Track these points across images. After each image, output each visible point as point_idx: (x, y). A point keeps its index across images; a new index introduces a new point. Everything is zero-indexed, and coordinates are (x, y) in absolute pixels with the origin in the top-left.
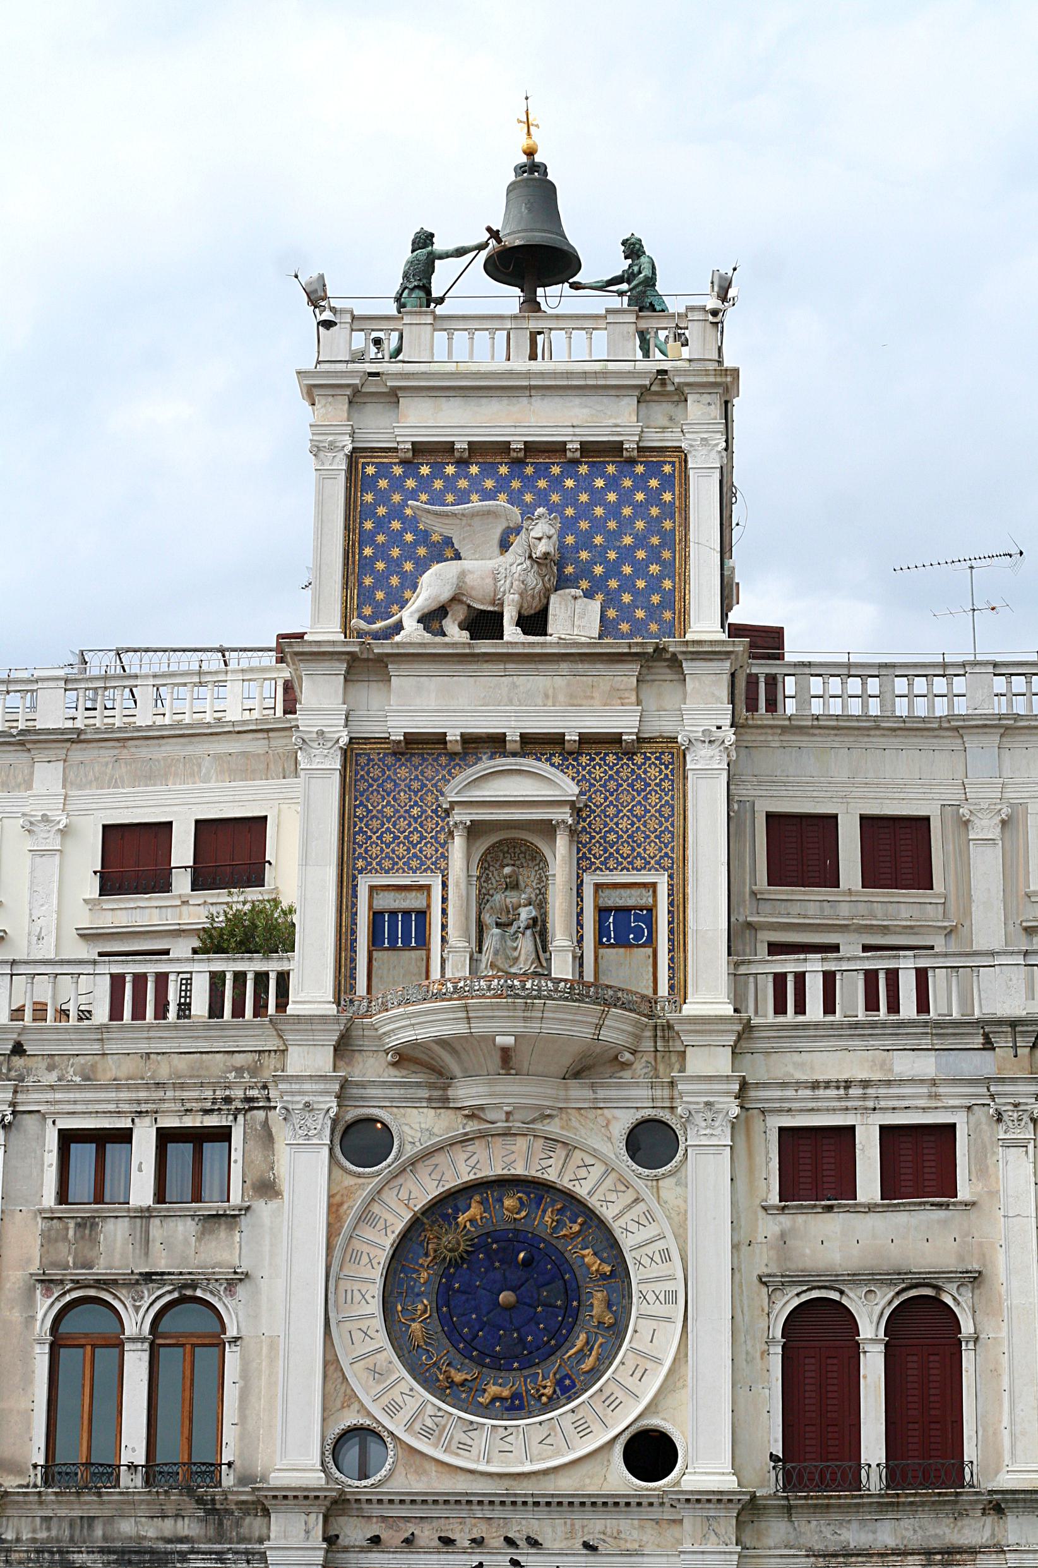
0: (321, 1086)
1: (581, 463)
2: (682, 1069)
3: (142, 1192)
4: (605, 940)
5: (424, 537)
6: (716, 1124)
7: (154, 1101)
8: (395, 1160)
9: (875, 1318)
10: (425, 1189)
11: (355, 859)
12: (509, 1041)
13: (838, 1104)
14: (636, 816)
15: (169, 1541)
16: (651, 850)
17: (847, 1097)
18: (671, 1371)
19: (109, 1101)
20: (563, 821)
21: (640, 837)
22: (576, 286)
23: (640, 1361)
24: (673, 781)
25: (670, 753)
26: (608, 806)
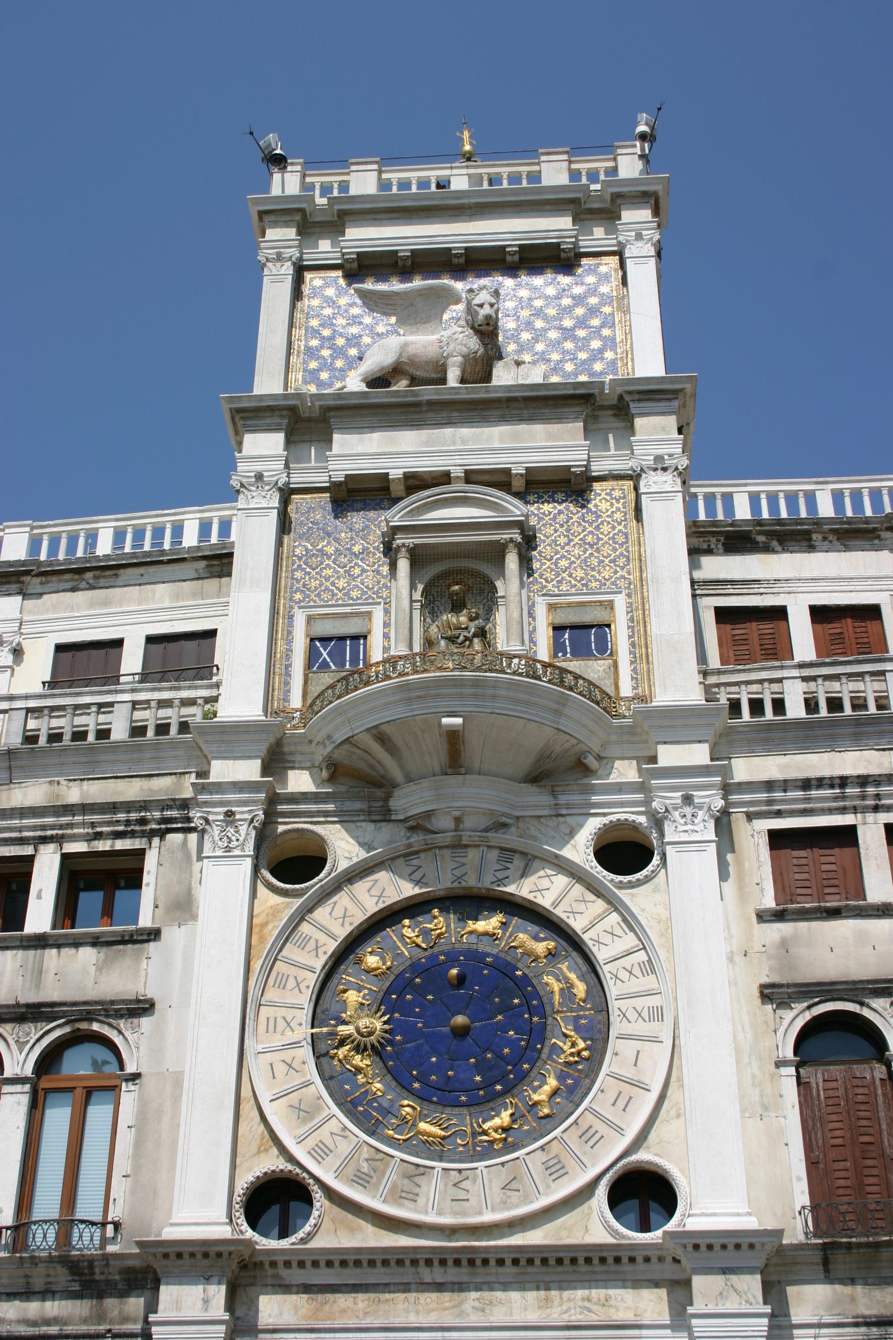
4: (560, 654)
7: (61, 827)
15: (34, 1324)
17: (844, 797)
20: (511, 540)
26: (559, 536)
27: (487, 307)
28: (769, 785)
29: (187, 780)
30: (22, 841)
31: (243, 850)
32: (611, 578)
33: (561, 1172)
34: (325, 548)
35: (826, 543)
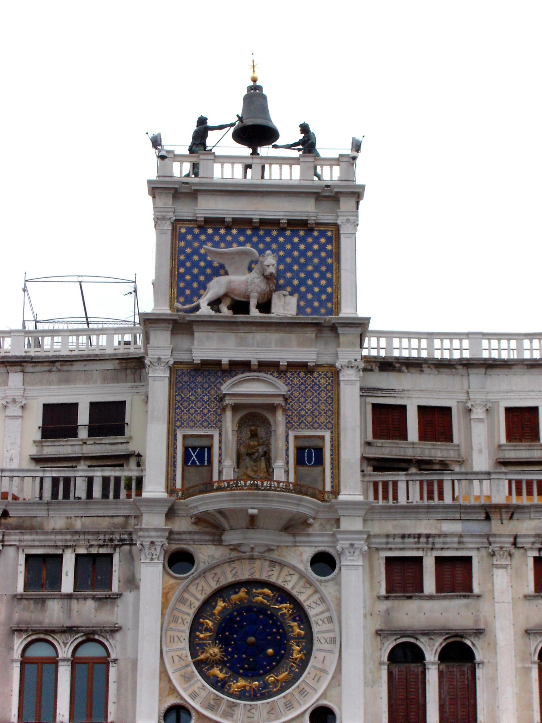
0: (159, 534)
1: (287, 230)
2: (338, 527)
3: (67, 584)
5: (209, 264)
6: (356, 554)
9: (434, 652)
10: (210, 585)
12: (255, 511)
16: (322, 419)
17: (418, 542)
18: (333, 677)
19: (51, 540)
21: (316, 413)
22: (275, 147)
23: (318, 672)
24: (332, 386)
25: (331, 372)
27: (271, 267)
28: (388, 536)
30: (56, 547)
31: (158, 560)
33: (291, 707)
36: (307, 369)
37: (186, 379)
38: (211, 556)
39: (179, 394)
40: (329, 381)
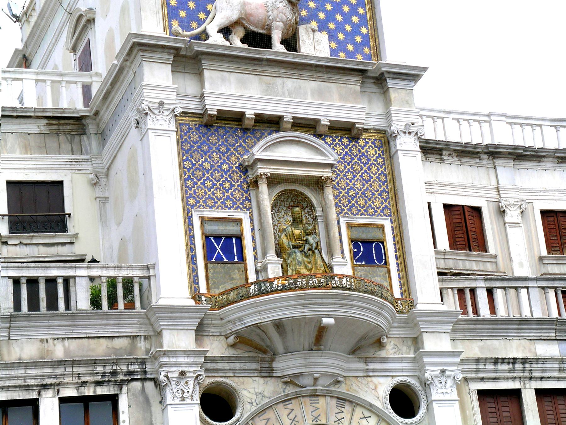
0: (191, 359)
7: (56, 377)
8: (242, 415)
11: (187, 198)
13: (508, 374)
14: (365, 180)
19: (17, 378)
21: (369, 194)
29: (139, 341)
30: (28, 387)
32: (380, 207)
34: (204, 164)
35: (450, 158)
36: (350, 134)
37: (195, 137)
38: (260, 393)
39: (187, 159)
40: (379, 152)
